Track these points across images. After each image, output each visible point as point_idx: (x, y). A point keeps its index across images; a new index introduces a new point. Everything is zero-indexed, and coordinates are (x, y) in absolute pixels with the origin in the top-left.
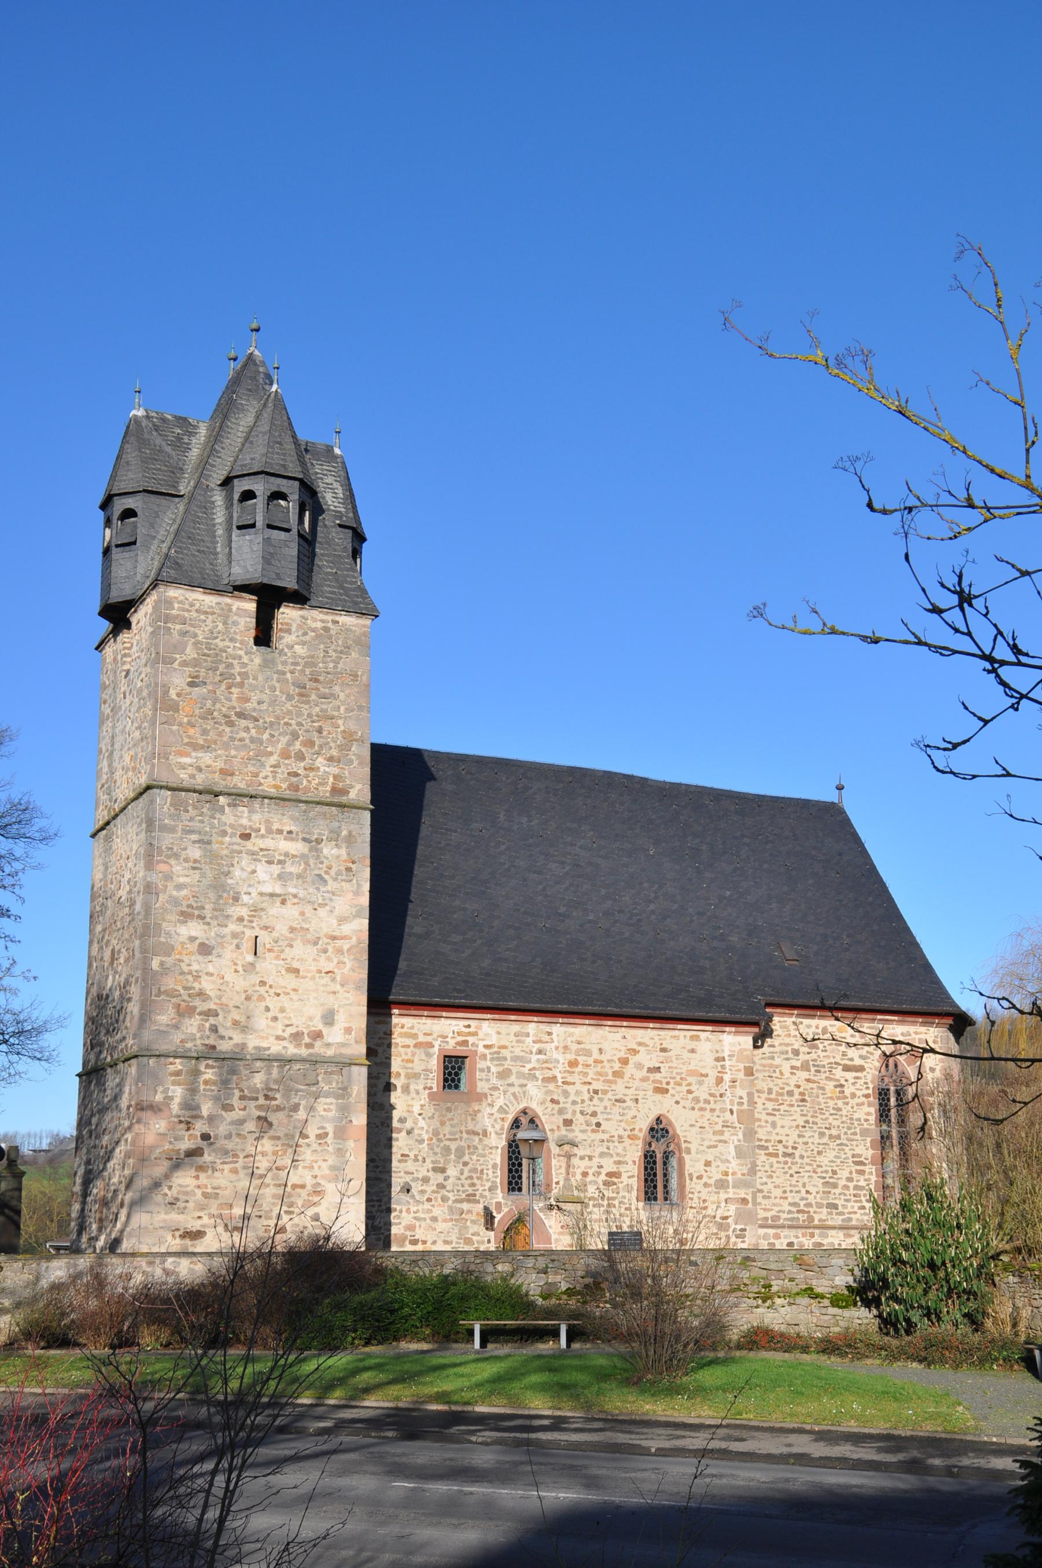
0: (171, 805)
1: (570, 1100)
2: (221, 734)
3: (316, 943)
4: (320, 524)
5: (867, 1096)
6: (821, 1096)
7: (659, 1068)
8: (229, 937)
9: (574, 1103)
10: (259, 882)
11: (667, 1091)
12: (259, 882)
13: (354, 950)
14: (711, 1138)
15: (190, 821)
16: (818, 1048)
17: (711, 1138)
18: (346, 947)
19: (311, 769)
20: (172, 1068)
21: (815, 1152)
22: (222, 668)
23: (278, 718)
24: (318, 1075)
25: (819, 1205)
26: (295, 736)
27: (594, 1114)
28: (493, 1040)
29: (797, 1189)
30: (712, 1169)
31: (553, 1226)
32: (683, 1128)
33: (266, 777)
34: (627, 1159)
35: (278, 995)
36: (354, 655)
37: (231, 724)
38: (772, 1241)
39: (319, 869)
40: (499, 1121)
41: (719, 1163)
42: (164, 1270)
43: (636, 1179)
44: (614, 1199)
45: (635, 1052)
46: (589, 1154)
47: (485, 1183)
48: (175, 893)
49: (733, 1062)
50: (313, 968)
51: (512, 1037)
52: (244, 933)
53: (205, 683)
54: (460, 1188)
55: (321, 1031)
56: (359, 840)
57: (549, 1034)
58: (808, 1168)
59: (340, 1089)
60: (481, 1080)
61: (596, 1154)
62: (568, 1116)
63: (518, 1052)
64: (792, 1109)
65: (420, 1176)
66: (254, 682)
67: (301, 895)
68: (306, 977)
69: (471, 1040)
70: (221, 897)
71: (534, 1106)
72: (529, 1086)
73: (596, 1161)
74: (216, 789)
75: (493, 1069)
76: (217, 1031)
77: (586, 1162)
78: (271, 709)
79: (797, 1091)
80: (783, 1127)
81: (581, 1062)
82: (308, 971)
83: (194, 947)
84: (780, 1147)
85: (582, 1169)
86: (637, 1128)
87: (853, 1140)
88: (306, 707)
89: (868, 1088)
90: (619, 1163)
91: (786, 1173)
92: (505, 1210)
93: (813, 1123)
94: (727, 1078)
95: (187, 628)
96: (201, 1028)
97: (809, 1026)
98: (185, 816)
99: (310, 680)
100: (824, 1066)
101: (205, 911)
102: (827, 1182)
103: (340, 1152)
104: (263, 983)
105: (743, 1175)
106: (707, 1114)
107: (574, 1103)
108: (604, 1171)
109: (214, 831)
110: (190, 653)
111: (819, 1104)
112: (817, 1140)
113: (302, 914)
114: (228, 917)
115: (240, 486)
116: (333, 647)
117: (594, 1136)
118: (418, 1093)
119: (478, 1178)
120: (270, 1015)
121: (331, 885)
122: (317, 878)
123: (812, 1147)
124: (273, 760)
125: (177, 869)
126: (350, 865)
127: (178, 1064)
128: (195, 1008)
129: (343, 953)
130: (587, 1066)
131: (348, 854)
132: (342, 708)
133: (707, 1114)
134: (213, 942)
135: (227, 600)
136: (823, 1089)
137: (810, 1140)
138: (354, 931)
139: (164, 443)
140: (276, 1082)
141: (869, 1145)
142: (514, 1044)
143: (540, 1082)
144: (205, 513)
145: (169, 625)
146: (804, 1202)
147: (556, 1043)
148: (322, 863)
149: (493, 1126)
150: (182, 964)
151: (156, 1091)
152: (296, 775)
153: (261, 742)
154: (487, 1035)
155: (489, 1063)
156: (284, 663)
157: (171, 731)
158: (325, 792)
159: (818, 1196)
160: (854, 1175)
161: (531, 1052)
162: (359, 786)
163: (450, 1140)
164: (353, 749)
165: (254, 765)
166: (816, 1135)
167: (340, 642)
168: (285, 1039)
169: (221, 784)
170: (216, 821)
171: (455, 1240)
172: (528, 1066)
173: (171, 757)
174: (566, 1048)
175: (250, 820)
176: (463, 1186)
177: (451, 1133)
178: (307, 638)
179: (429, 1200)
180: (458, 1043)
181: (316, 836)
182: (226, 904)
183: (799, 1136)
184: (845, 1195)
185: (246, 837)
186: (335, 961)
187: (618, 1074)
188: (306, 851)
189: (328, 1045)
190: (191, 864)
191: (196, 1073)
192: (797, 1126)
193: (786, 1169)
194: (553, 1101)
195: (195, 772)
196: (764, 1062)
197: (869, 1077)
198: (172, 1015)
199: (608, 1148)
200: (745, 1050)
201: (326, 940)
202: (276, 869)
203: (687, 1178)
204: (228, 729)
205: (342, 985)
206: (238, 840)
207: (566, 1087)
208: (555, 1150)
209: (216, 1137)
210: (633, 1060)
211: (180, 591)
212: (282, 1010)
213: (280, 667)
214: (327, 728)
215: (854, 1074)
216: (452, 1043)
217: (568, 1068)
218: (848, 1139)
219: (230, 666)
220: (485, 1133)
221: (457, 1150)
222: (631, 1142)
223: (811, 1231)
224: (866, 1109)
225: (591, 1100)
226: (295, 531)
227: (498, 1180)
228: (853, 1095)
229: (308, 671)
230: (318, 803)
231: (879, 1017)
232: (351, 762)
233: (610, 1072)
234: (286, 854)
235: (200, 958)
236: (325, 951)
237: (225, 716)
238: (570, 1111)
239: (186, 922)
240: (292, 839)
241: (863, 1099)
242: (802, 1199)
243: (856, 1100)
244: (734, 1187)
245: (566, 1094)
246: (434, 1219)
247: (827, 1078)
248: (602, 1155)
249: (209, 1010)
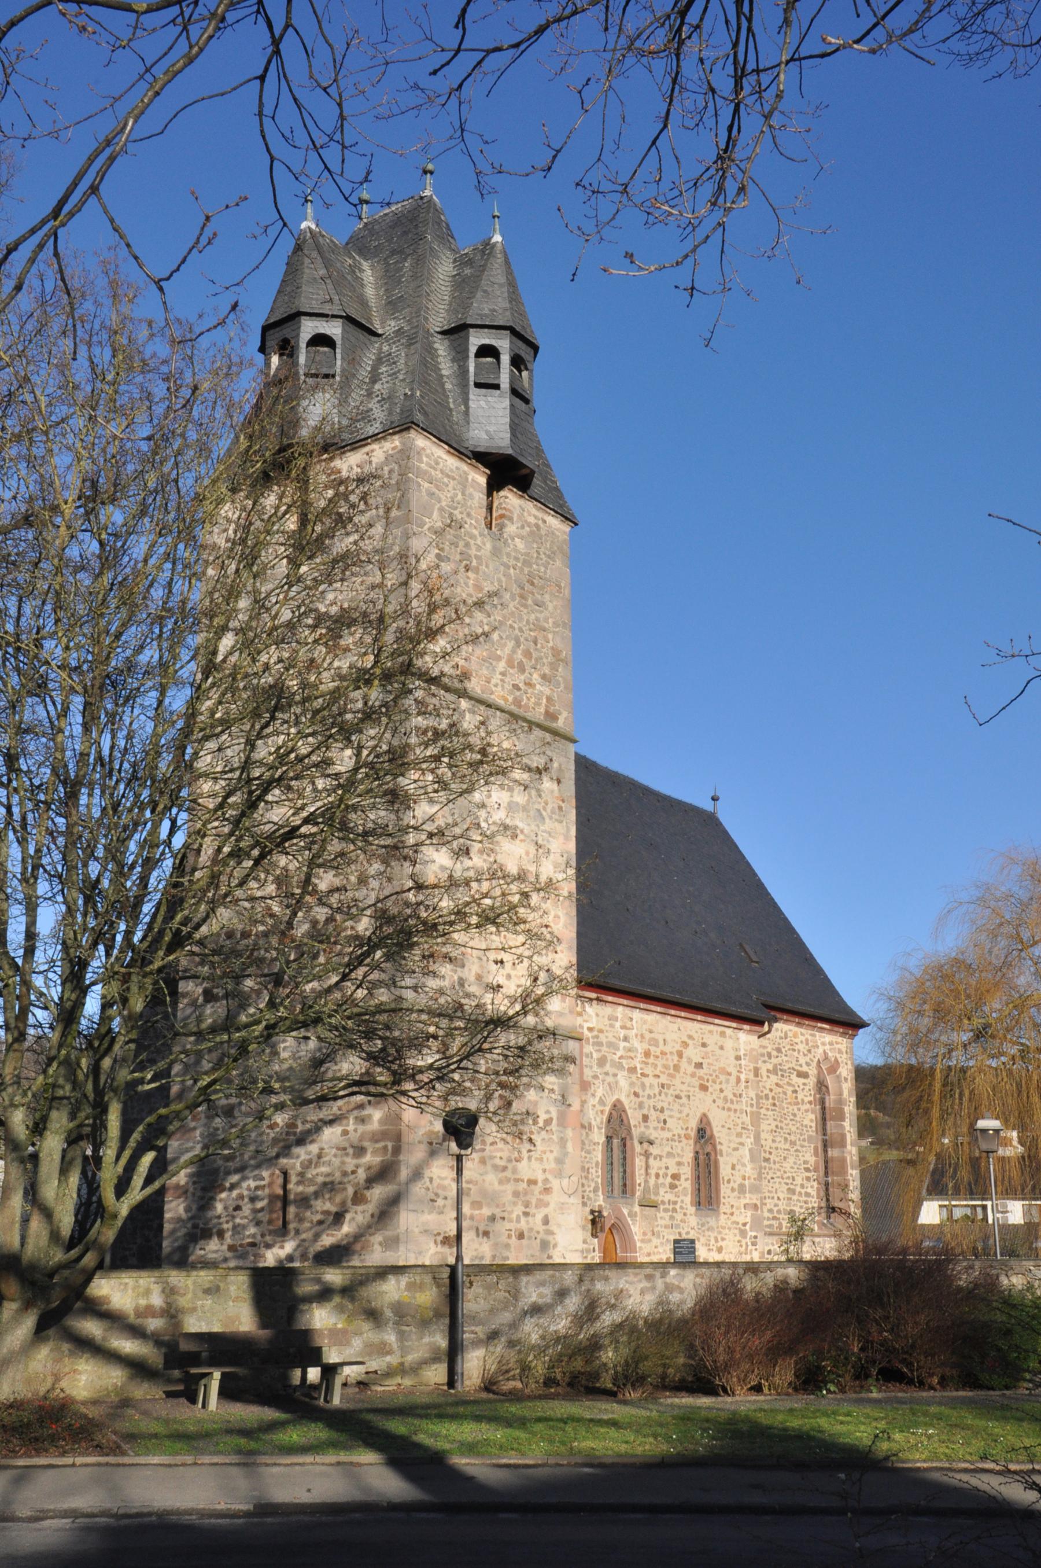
27: (662, 1110)
33: (496, 686)
42: (666, 1284)
53: (449, 559)
61: (664, 1154)
71: (623, 1099)
103: (563, 1142)
115: (476, 340)
135: (464, 467)
156: (508, 555)
208: (638, 1148)
213: (505, 559)
219: (467, 545)
241: (808, 1106)
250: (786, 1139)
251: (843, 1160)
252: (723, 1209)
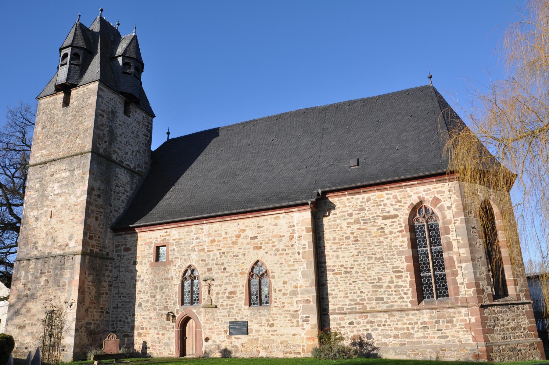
1: (211, 259)
3: (69, 209)
5: (401, 232)
6: (368, 237)
7: (257, 236)
9: (213, 260)
11: (261, 248)
14: (286, 269)
16: (365, 210)
17: (286, 269)
21: (366, 269)
25: (370, 299)
27: (222, 264)
28: (176, 236)
29: (354, 291)
30: (288, 285)
31: (202, 320)
32: (270, 266)
34: (240, 284)
38: (339, 322)
40: (178, 272)
41: (292, 282)
43: (244, 294)
44: (232, 305)
45: (244, 231)
46: (220, 284)
47: (172, 301)
48: (31, 201)
49: (299, 227)
50: (67, 219)
51: (185, 234)
54: (161, 304)
57: (202, 229)
58: (362, 278)
60: (171, 255)
61: (223, 283)
62: (210, 267)
63: (187, 240)
64: (350, 246)
65: (146, 300)
69: (167, 238)
70: (43, 199)
71: (195, 264)
72: (192, 254)
73: (224, 287)
75: (176, 249)
77: (218, 288)
79: (352, 236)
80: (343, 257)
81: (217, 240)
84: (342, 268)
85: (217, 291)
86: (245, 268)
87: (392, 259)
89: (401, 227)
90: (235, 287)
91: (347, 283)
92: (180, 313)
93: (364, 252)
94: (296, 236)
97: (358, 199)
100: (370, 219)
102: (375, 286)
105: (307, 287)
106: (284, 256)
107: (213, 260)
108: (227, 292)
111: (367, 241)
112: (366, 261)
113: (66, 199)
117: (222, 275)
118: (145, 264)
119: (169, 299)
121: (76, 185)
123: (363, 266)
126: (83, 175)
130: (219, 241)
133: (284, 256)
135: (56, 96)
136: (370, 232)
137: (362, 263)
141: (404, 260)
142: (186, 236)
143: (197, 252)
146: (360, 298)
147: (205, 233)
149: (176, 275)
154: (174, 234)
155: (174, 247)
159: (369, 294)
160: (394, 279)
161: (193, 239)
162: (88, 145)
163: (157, 283)
166: (366, 259)
171: (158, 326)
172: (192, 246)
174: (210, 234)
176: (162, 303)
177: (158, 280)
178: (78, 98)
179: (149, 310)
180: (162, 240)
183: (354, 261)
184: (388, 291)
185: (52, 175)
187: (234, 243)
189: (70, 248)
192: (353, 256)
193: (347, 281)
194: (202, 260)
196: (330, 223)
197: (402, 220)
199: (230, 280)
200: (306, 219)
202: (60, 184)
203: (273, 291)
205: (76, 223)
206: (50, 177)
207: (209, 253)
210: (243, 235)
211: (44, 100)
215: (391, 220)
216: (159, 240)
217: (210, 244)
218: (388, 259)
220: (172, 278)
221: (160, 287)
222: (241, 275)
223: (365, 314)
224: (401, 239)
225: (221, 257)
227: (177, 299)
228: (391, 233)
231: (403, 184)
233: (231, 243)
235: (35, 223)
238: (211, 264)
242: (358, 296)
243: (393, 235)
244: (301, 294)
245: (209, 256)
246: (151, 318)
247: (372, 226)
248: (226, 284)
250: (370, 258)
251: (451, 259)
252: (273, 304)
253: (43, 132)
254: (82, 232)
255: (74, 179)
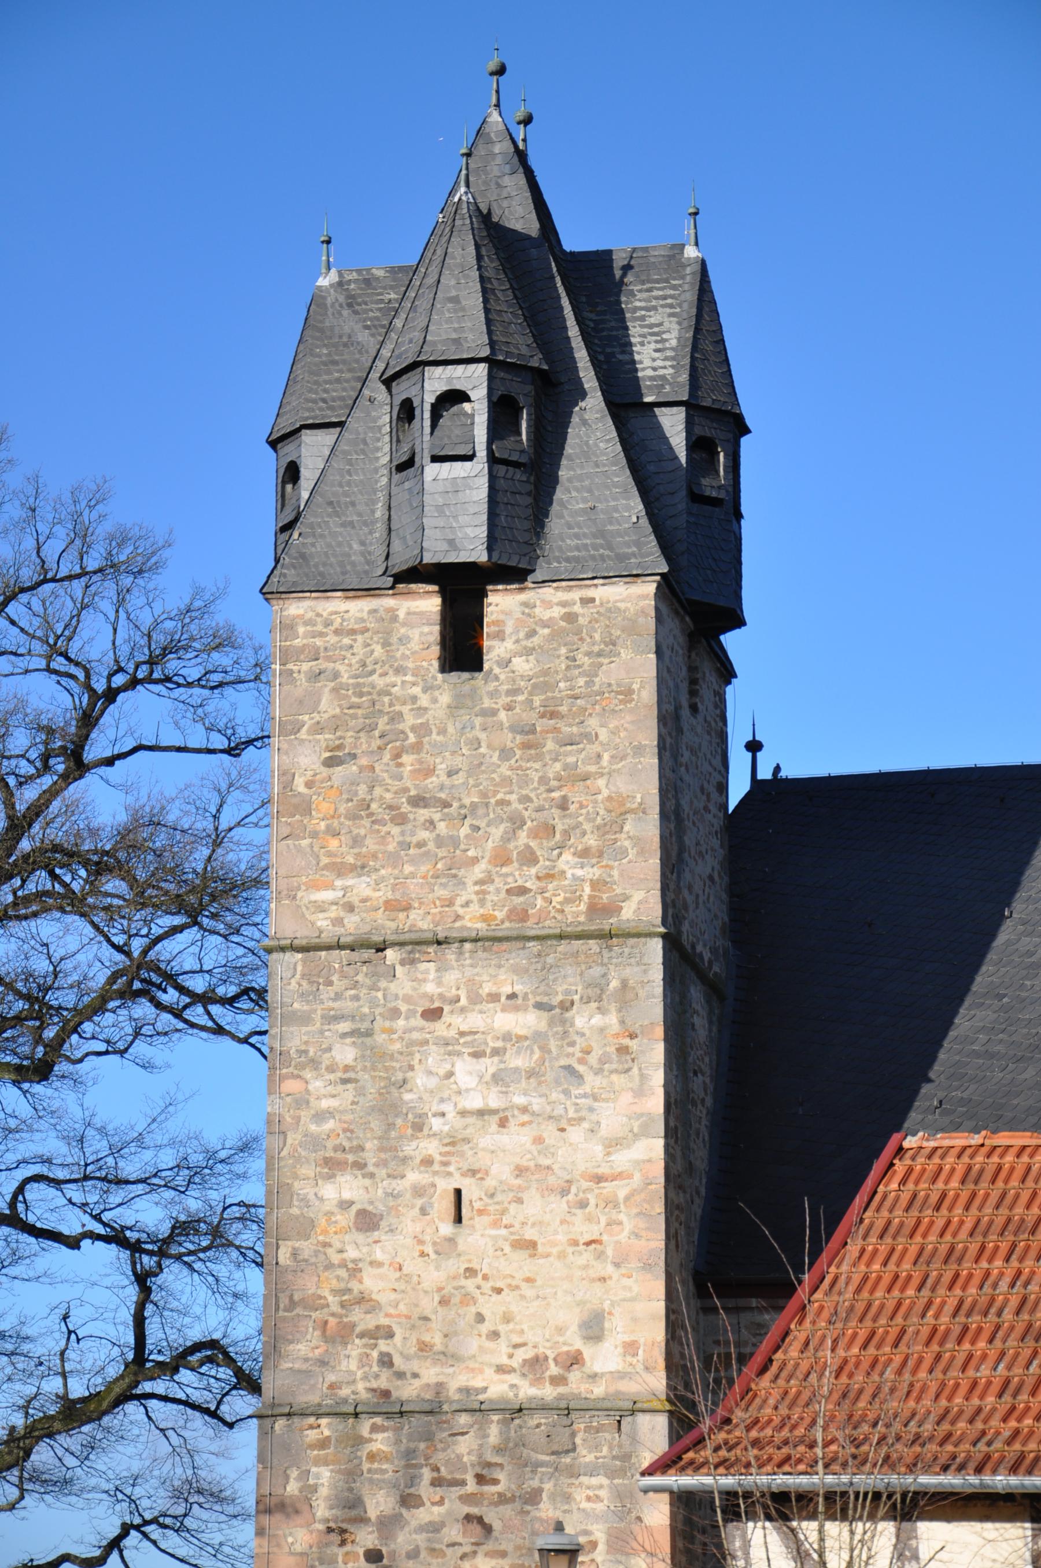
0: (303, 976)
2: (383, 840)
3: (564, 1192)
4: (575, 419)
8: (408, 1195)
10: (460, 1093)
12: (460, 1093)
13: (638, 1198)
15: (334, 1000)
18: (622, 1194)
19: (550, 877)
20: (312, 1435)
22: (382, 723)
23: (484, 795)
24: (573, 1435)
26: (517, 822)
33: (467, 904)
35: (499, 1291)
36: (625, 654)
37: (401, 819)
39: (568, 1055)
48: (313, 1128)
50: (562, 1238)
52: (434, 1185)
53: (354, 756)
55: (579, 1353)
56: (642, 993)
59: (614, 1458)
66: (440, 738)
67: (536, 1108)
68: (548, 1255)
70: (391, 1126)
74: (377, 938)
76: (391, 1364)
78: (471, 781)
82: (553, 1244)
83: (344, 1219)
88: (537, 765)
95: (322, 664)
96: (364, 1360)
98: (327, 993)
99: (542, 716)
101: (366, 1155)
104: (471, 1272)
109: (378, 1011)
110: (328, 706)
113: (539, 1140)
114: (405, 1160)
116: (585, 648)
120: (485, 1328)
121: (592, 1082)
122: (563, 1073)
124: (478, 871)
125: (317, 1085)
126: (627, 1041)
127: (326, 1427)
128: (353, 1326)
129: (616, 1206)
131: (622, 1022)
132: (606, 757)
134: (381, 1207)
135: (389, 602)
138: (637, 1162)
139: (358, 327)
140: (499, 1450)
144: (363, 452)
145: (290, 666)
148: (572, 1044)
150: (330, 1251)
151: (287, 1478)
152: (523, 891)
153: (455, 842)
156: (492, 695)
157: (299, 849)
158: (577, 914)
162: (638, 896)
164: (626, 828)
165: (444, 886)
167: (597, 637)
168: (514, 1370)
169: (387, 926)
170: (380, 995)
173: (300, 894)
175: (439, 984)
178: (536, 640)
181: (560, 998)
182: (401, 1137)
185: (433, 1014)
186: (603, 1220)
188: (543, 1026)
189: (594, 1377)
190: (340, 1074)
191: (359, 1441)
195: (342, 914)
198: (314, 1343)
201: (585, 1184)
202: (489, 1065)
204: (396, 830)
205: (617, 1265)
206: (419, 1022)
209: (393, 1554)
211: (307, 603)
212: (507, 1319)
213: (487, 703)
214: (576, 795)
219: (396, 717)
226: (482, 453)
229: (537, 701)
230: (561, 937)
232: (625, 852)
234: (507, 1037)
235: (360, 1237)
236: (583, 1205)
237: (390, 807)
239: (333, 1176)
240: (517, 1009)
249: (378, 1327)
253: (336, 781)
254: (660, 1307)
255: (576, 1050)
